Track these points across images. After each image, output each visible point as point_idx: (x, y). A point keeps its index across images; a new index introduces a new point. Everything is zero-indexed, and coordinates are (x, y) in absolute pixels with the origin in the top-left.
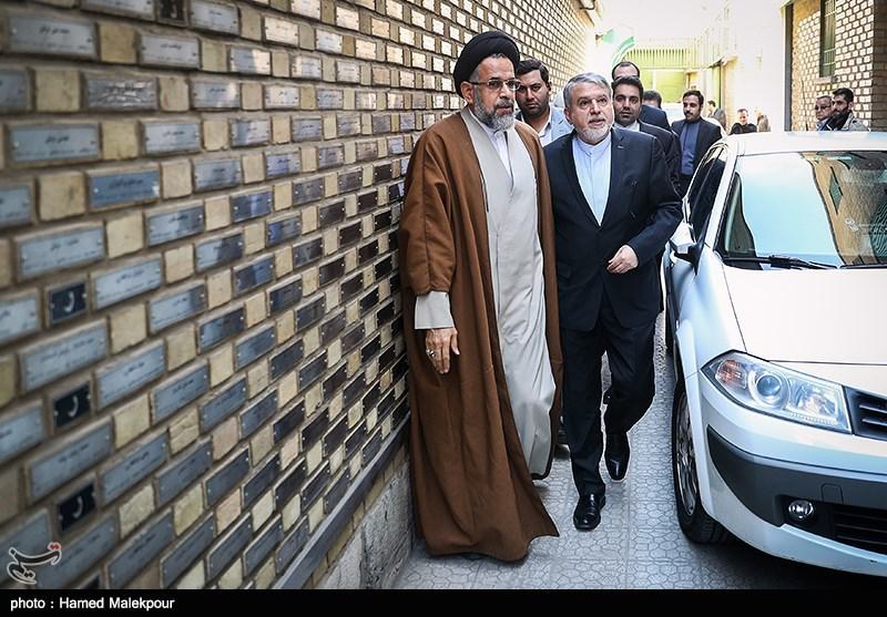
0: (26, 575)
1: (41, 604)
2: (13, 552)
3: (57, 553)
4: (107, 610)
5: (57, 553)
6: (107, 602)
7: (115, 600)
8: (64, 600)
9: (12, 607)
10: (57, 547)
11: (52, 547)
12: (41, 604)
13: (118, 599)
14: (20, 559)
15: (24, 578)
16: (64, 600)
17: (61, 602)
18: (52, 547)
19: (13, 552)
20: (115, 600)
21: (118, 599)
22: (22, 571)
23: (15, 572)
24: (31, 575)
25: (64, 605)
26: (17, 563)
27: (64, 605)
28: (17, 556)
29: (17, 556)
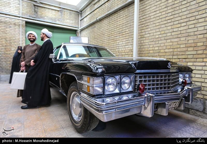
0: (6, 134)
1: (11, 141)
2: (3, 129)
3: (14, 129)
4: (33, 142)
5: (14, 129)
6: (33, 141)
7: (34, 140)
8: (20, 140)
9: (3, 142)
10: (14, 128)
11: (12, 128)
12: (11, 141)
13: (35, 140)
14: (5, 130)
15: (5, 134)
16: (20, 140)
17: (20, 141)
18: (12, 128)
19: (3, 129)
20: (34, 140)
21: (35, 140)
22: (5, 133)
23: (4, 133)
24: (7, 134)
25: (20, 141)
26: (6, 132)
27: (20, 141)
28: (4, 130)
29: (4, 130)
